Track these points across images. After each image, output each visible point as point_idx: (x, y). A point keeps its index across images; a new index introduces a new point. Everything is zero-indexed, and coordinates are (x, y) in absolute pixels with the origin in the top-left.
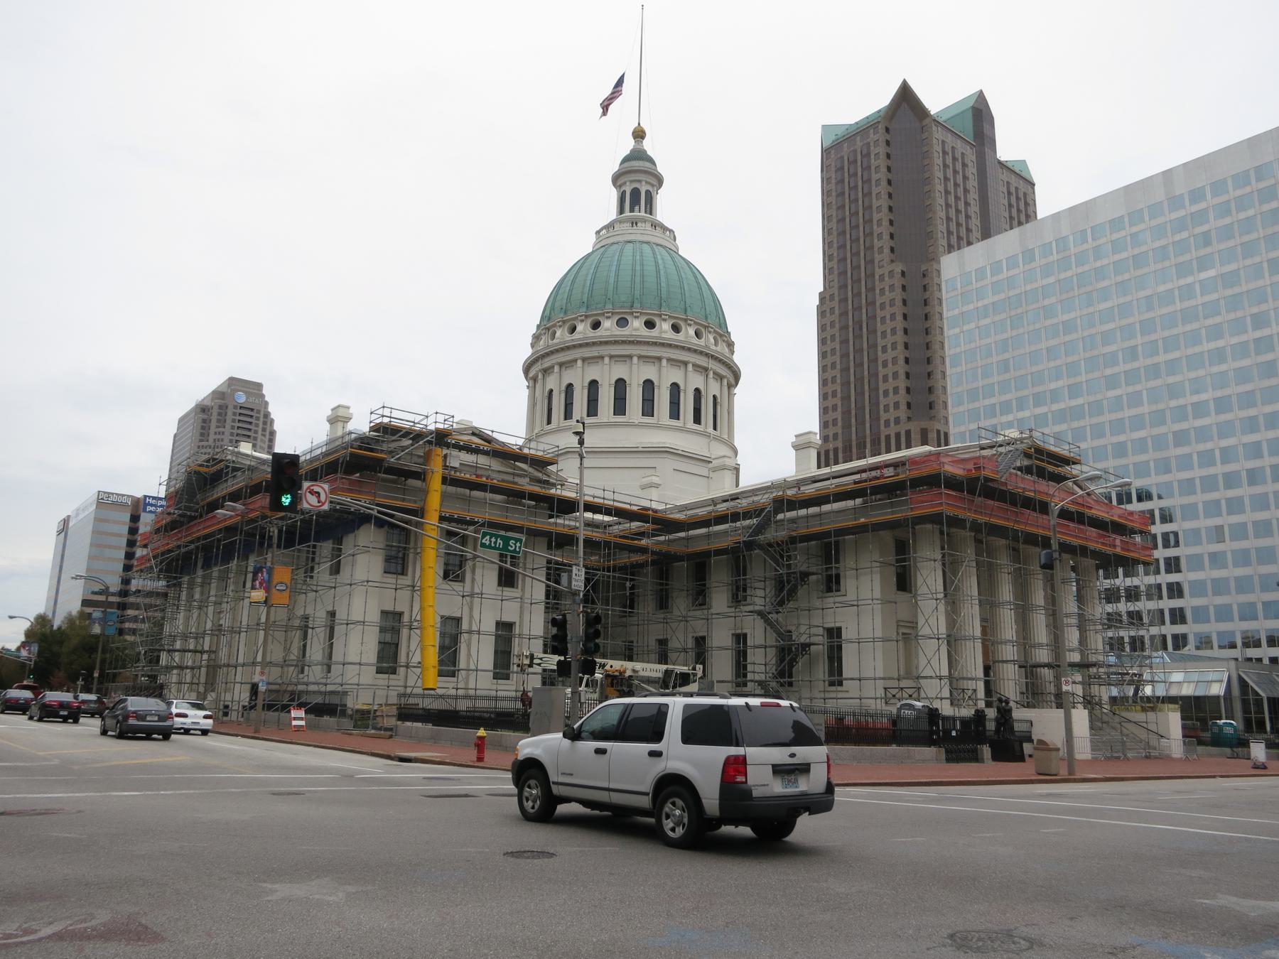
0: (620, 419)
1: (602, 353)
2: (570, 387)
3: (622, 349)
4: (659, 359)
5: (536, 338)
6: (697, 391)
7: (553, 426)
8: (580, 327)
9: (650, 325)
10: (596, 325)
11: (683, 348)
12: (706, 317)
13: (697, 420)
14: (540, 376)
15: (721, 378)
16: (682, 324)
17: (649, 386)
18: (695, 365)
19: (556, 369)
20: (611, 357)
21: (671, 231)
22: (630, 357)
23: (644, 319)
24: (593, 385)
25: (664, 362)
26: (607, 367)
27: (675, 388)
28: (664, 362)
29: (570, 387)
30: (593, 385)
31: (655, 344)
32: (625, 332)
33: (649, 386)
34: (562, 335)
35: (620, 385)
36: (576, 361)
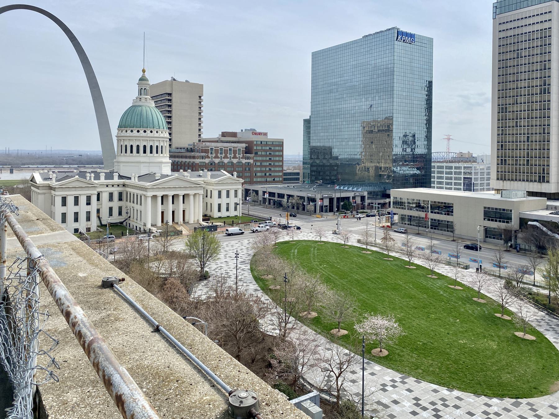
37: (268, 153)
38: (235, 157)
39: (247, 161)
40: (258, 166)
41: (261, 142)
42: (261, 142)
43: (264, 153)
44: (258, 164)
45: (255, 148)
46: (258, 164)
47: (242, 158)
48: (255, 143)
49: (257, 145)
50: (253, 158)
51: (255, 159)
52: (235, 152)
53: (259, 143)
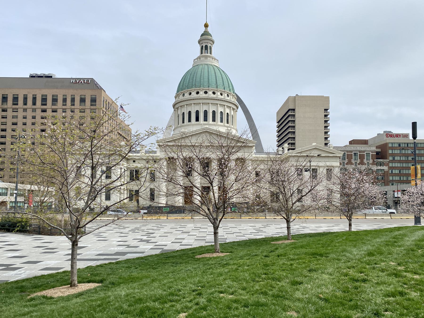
0: (197, 122)
1: (192, 103)
2: (184, 113)
3: (197, 101)
4: (209, 103)
5: (176, 97)
6: (221, 112)
7: (179, 125)
8: (186, 95)
9: (206, 93)
10: (190, 94)
11: (216, 100)
12: (224, 88)
13: (222, 121)
14: (176, 110)
15: (230, 107)
16: (216, 92)
17: (206, 112)
18: (220, 104)
19: (180, 108)
20: (194, 104)
21: (217, 60)
22: (200, 103)
23: (204, 91)
24: (190, 113)
25: (210, 104)
26: (193, 107)
27: (214, 112)
28: (210, 104)
29: (184, 113)
30: (190, 113)
31: (207, 99)
32: (198, 95)
33: (206, 112)
34: (181, 97)
35: (197, 112)
36: (184, 105)
37: (410, 158)
38: (362, 163)
39: (379, 168)
40: (396, 175)
41: (399, 145)
42: (399, 145)
43: (403, 158)
44: (397, 172)
45: (390, 152)
46: (397, 172)
47: (373, 164)
48: (390, 145)
49: (392, 148)
50: (388, 165)
51: (391, 165)
52: (362, 157)
53: (396, 145)
